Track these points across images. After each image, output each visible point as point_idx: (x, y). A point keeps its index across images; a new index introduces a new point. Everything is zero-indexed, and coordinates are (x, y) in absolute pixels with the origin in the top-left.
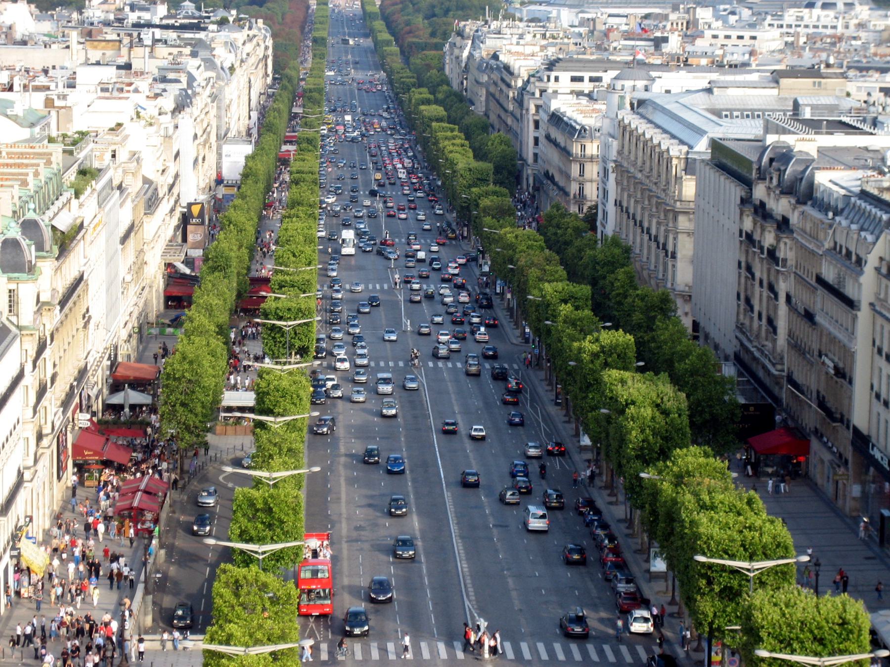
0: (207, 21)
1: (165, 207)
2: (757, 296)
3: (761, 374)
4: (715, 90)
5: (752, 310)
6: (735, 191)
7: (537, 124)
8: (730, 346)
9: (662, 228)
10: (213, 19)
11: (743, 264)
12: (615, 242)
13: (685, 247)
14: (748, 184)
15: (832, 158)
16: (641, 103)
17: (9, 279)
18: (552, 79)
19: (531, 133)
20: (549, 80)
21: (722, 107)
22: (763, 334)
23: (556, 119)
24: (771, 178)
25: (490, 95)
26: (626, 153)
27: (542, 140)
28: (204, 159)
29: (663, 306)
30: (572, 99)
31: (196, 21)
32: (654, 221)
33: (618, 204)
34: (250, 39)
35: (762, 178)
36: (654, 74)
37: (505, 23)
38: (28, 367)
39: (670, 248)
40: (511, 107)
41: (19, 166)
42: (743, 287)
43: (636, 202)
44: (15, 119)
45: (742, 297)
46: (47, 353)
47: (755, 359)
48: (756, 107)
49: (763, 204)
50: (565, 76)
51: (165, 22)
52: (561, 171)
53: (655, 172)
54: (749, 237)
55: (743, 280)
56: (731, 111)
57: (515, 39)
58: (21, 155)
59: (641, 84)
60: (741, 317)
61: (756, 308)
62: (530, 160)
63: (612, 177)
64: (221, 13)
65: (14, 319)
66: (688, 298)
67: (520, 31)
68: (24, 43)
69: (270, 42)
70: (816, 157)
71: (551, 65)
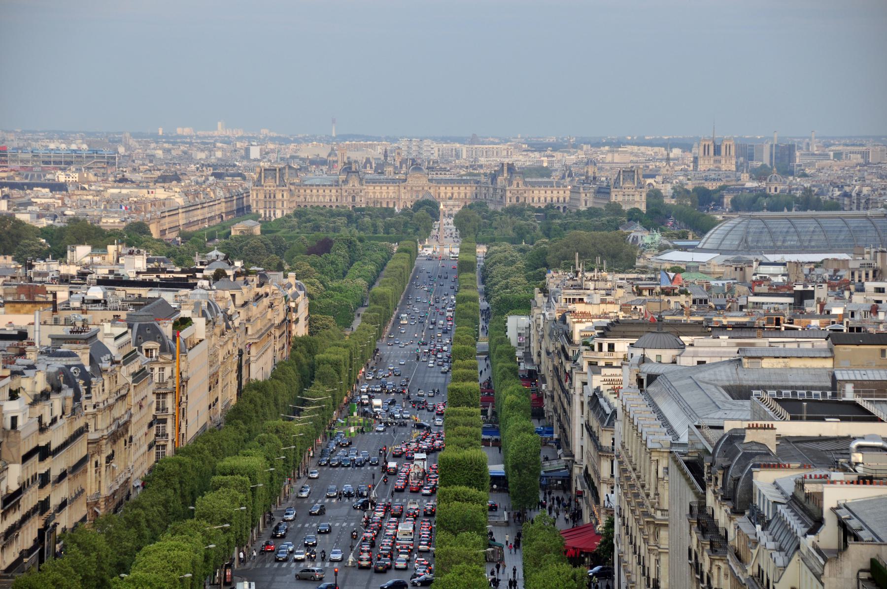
0: (199, 275)
4: (745, 360)
10: (206, 273)
16: (652, 378)
18: (605, 347)
20: (601, 349)
21: (751, 383)
23: (595, 399)
24: (717, 479)
25: (556, 369)
28: (110, 458)
31: (184, 276)
34: (258, 298)
36: (686, 339)
37: (589, 275)
39: (652, 576)
48: (799, 384)
50: (622, 346)
51: (141, 277)
57: (597, 298)
59: (667, 355)
67: (609, 285)
69: (303, 303)
70: (774, 451)
71: (606, 331)
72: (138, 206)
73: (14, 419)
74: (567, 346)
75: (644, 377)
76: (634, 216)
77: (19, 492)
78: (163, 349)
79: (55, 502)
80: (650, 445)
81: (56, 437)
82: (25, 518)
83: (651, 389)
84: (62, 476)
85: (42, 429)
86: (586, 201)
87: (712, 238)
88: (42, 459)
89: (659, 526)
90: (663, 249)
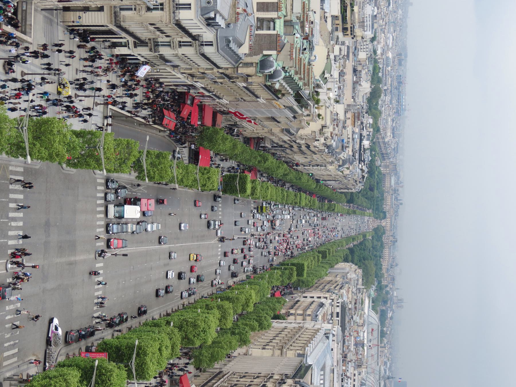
1: (286, 138)
2: (246, 380)
3: (213, 381)
5: (240, 378)
6: (290, 372)
7: (320, 298)
8: (225, 370)
9: (275, 344)
10: (364, 166)
11: (260, 375)
12: (269, 326)
13: (267, 353)
14: (294, 377)
16: (328, 338)
17: (257, 63)
18: (338, 304)
19: (315, 294)
22: (230, 382)
23: (322, 305)
26: (307, 331)
27: (312, 300)
29: (244, 342)
30: (330, 312)
32: (278, 341)
33: (285, 328)
34: (356, 181)
35: (296, 383)
38: (220, 71)
39: (267, 347)
40: (326, 288)
41: (304, 71)
42: (250, 375)
43: (286, 335)
44: (324, 73)
45: (246, 374)
46: (226, 80)
47: (220, 379)
49: (285, 383)
50: (338, 310)
51: (362, 146)
52: (300, 306)
53: (298, 342)
54: (271, 377)
55: (253, 375)
56: (324, 375)
58: (308, 75)
60: (238, 374)
61: (241, 380)
62: (304, 295)
63: (297, 325)
64: (366, 170)
65: (241, 65)
66: (245, 354)
68: (354, 88)
69: (353, 191)
72: (385, 129)
73: (318, 140)
74: (338, 287)
75: (328, 335)
76: (380, 282)
77: (296, 143)
78: (340, 166)
79: (293, 149)
80: (307, 348)
81: (312, 148)
82: (288, 144)
83: (324, 337)
84: (301, 150)
85: (315, 147)
86: (385, 265)
87: (373, 314)
88: (306, 147)
89: (281, 350)
90: (369, 297)
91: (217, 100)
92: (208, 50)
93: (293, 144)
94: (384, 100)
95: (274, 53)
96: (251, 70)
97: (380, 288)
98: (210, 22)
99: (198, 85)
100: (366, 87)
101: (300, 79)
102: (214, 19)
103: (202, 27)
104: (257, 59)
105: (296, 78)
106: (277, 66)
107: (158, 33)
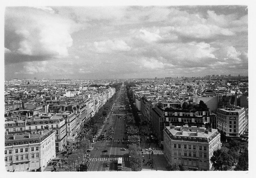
1: (98, 103)
15: (149, 98)
91: (86, 118)
92: (70, 121)
93: (100, 102)
94: (98, 84)
95: (73, 107)
96: (76, 111)
97: (136, 83)
98: (61, 120)
99: (81, 122)
100: (94, 88)
101: (80, 101)
102: (60, 120)
103: (62, 122)
104: (74, 110)
105: (80, 102)
106: (76, 106)
107: (64, 131)
